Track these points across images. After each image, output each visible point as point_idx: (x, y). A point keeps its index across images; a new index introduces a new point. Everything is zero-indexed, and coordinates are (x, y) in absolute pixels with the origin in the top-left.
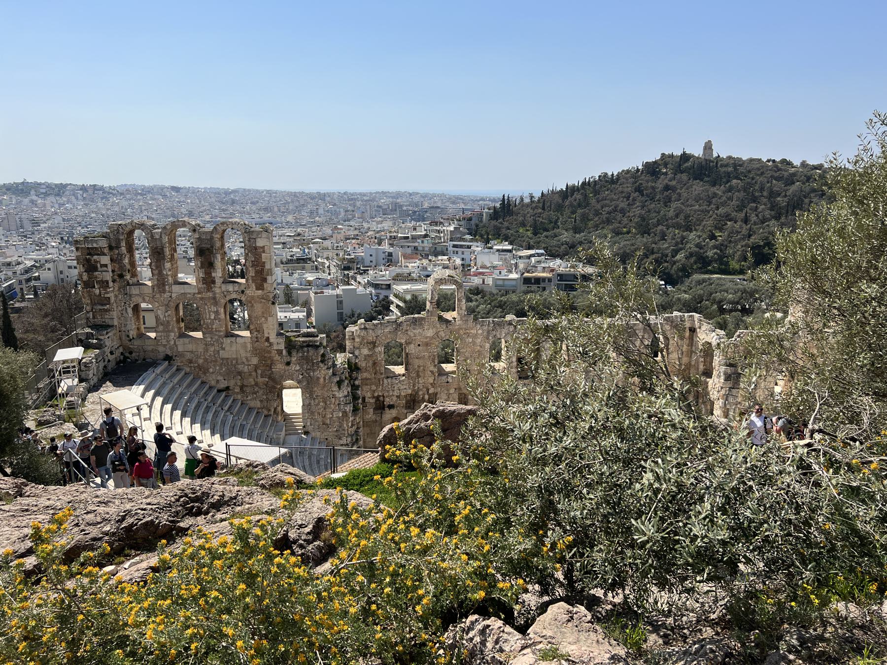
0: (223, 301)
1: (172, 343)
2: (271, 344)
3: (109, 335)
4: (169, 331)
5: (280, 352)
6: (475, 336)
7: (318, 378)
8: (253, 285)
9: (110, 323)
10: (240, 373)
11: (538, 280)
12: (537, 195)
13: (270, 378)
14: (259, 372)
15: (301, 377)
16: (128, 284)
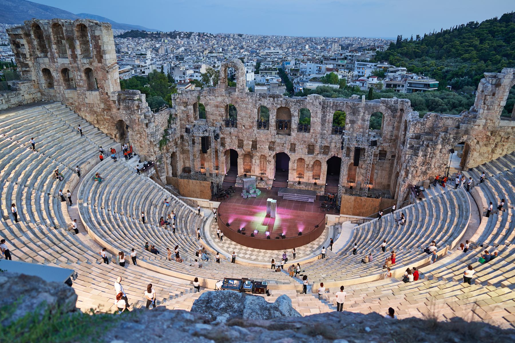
0: (82, 69)
1: (62, 92)
2: (109, 97)
3: (25, 84)
4: (60, 85)
5: (114, 102)
6: (247, 104)
7: (135, 119)
8: (96, 60)
9: (30, 79)
10: (96, 112)
11: (395, 86)
12: (422, 36)
13: (111, 117)
14: (105, 112)
15: (126, 118)
16: (38, 57)
